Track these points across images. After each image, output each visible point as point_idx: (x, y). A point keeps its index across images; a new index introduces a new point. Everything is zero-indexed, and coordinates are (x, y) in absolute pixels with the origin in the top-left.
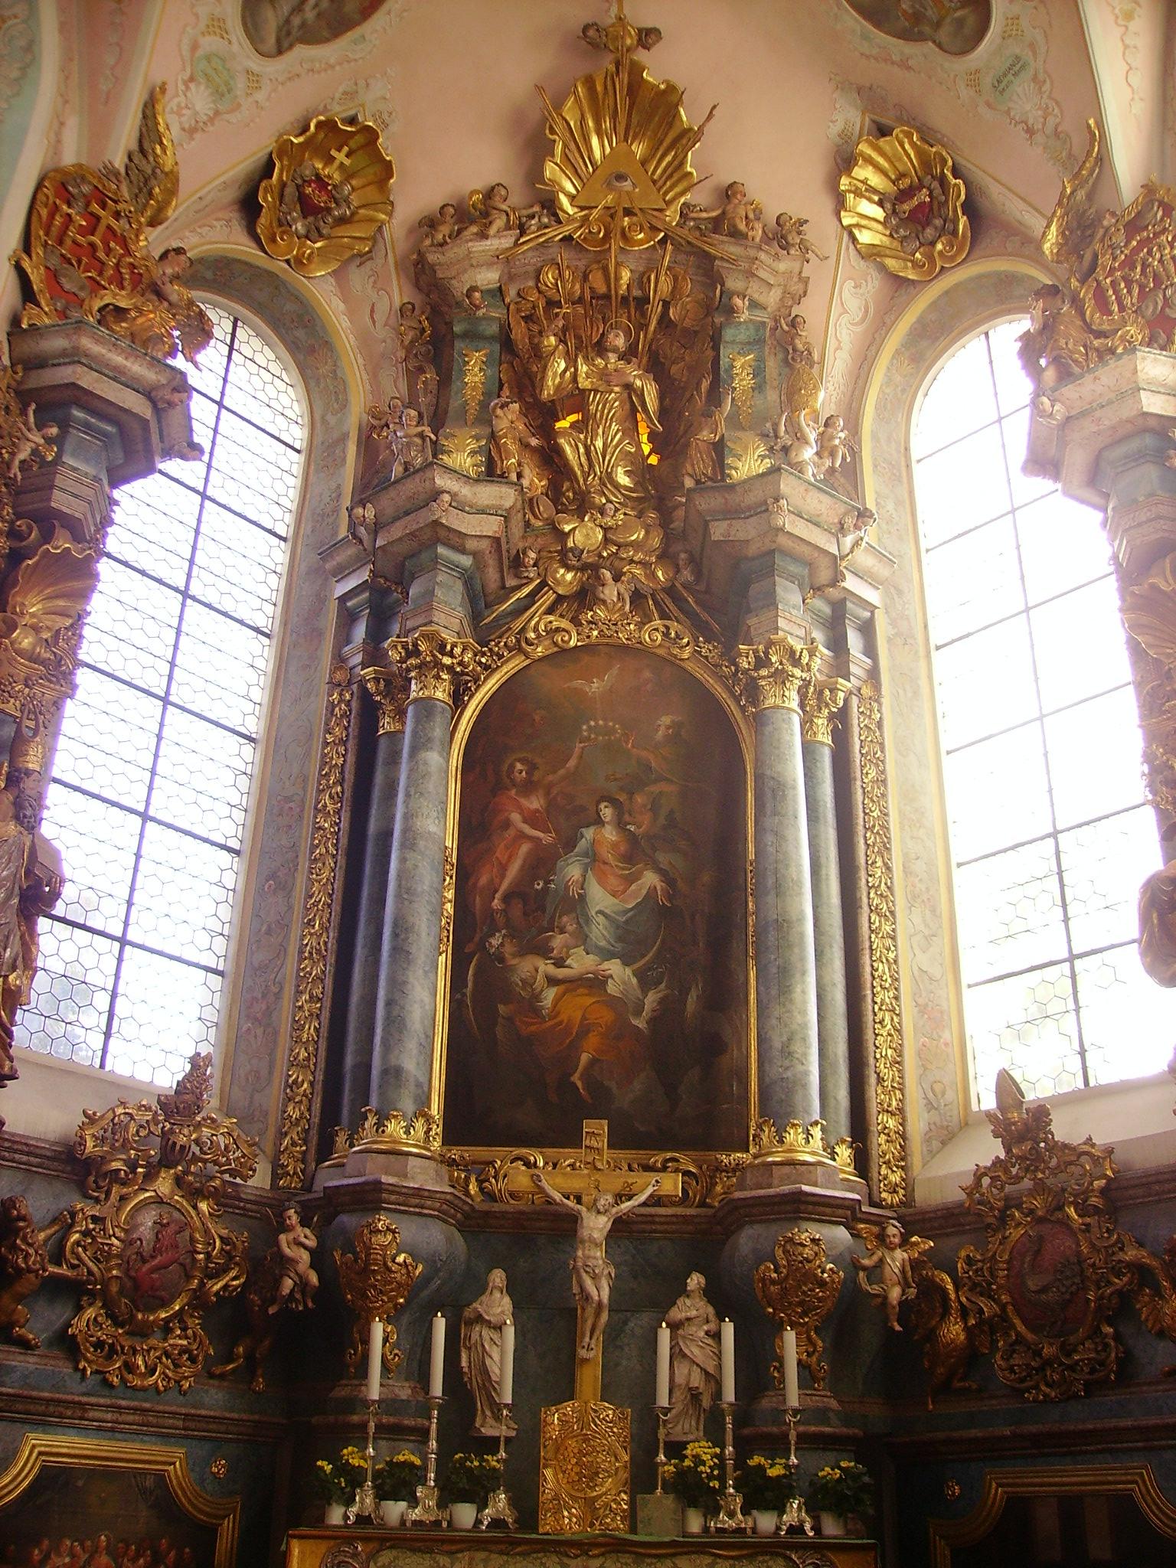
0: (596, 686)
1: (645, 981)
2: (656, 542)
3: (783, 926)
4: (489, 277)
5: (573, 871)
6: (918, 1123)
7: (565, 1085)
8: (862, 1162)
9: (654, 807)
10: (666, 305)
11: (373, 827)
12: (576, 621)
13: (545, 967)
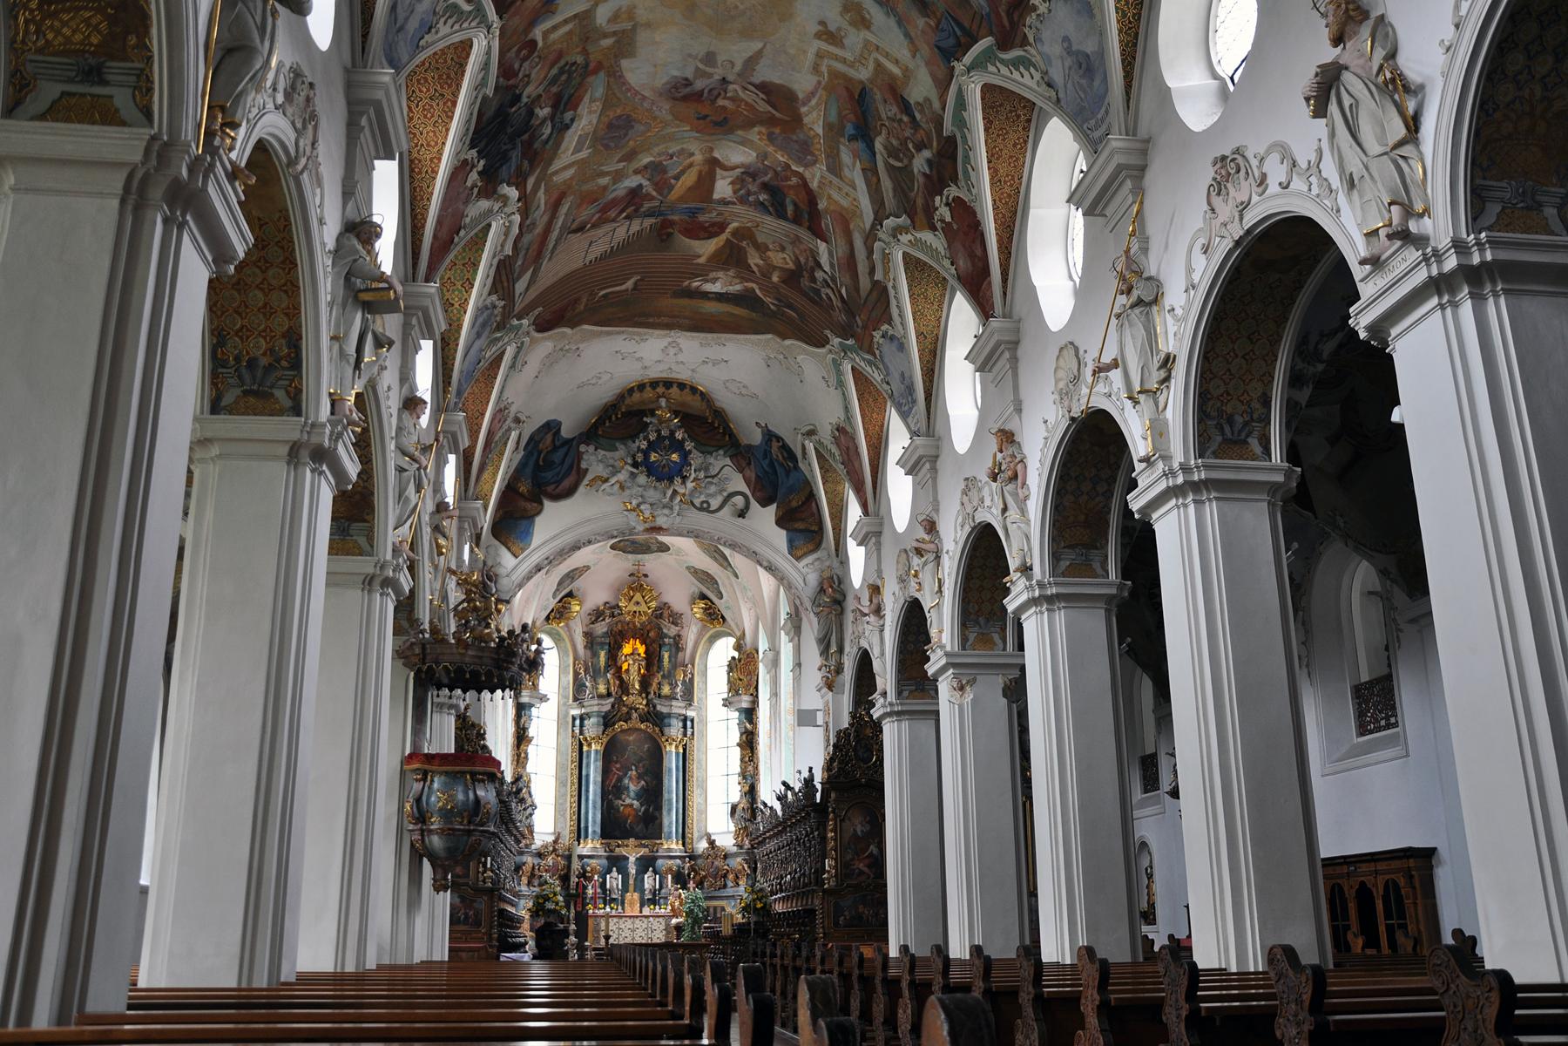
0: (631, 738)
1: (642, 805)
2: (644, 702)
3: (670, 800)
4: (605, 630)
5: (627, 781)
6: (696, 835)
7: (625, 827)
8: (684, 845)
9: (644, 766)
10: (648, 632)
11: (584, 773)
12: (626, 722)
13: (621, 802)
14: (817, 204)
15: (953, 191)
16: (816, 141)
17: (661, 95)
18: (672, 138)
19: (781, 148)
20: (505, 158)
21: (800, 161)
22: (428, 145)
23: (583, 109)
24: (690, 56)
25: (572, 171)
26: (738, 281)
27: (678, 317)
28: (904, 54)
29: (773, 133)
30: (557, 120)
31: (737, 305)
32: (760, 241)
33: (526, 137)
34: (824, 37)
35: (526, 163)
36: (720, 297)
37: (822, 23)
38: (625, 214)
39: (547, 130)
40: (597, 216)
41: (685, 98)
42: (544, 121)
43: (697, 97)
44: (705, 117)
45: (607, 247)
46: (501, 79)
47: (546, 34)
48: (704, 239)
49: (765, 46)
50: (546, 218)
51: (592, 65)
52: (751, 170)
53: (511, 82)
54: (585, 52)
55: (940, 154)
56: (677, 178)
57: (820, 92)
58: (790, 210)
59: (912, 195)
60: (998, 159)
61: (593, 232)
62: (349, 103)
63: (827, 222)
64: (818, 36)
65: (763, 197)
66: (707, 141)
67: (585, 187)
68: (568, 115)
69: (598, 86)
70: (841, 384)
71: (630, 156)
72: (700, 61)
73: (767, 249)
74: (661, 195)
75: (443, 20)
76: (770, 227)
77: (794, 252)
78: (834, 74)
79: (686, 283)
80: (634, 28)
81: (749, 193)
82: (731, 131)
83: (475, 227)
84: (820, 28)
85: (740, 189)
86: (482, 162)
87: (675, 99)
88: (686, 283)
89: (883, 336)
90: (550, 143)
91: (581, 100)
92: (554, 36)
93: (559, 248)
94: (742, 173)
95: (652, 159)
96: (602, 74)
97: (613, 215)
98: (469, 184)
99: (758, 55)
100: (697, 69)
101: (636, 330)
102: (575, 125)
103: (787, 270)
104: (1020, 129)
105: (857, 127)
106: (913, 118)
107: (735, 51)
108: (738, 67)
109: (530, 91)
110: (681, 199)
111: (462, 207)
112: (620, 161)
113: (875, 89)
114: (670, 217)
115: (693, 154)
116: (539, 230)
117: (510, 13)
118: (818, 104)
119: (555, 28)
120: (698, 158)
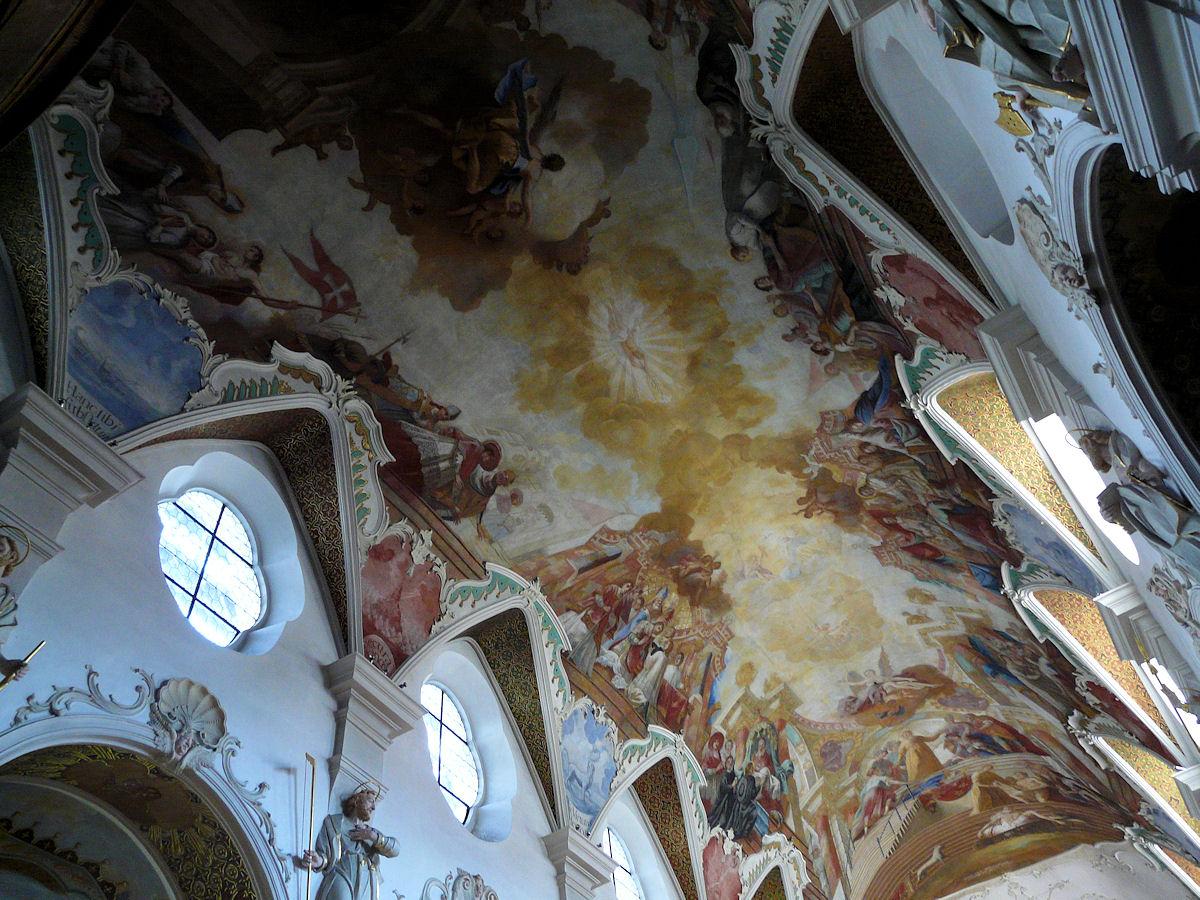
15: (1081, 681)
16: (974, 689)
17: (842, 717)
18: (874, 740)
19: (956, 707)
20: (751, 819)
21: (976, 707)
22: (676, 842)
23: (793, 753)
25: (818, 801)
26: (1015, 814)
27: (998, 862)
28: (970, 602)
30: (778, 772)
31: (1033, 832)
33: (759, 796)
34: (914, 621)
35: (775, 813)
36: (1016, 832)
37: (905, 613)
38: (887, 808)
39: (775, 782)
40: (866, 819)
41: (861, 709)
42: (767, 778)
43: (867, 705)
44: (886, 714)
45: (893, 837)
46: (709, 771)
47: (724, 724)
48: (962, 796)
49: (883, 649)
50: (824, 841)
51: (776, 725)
53: (718, 768)
54: (763, 719)
55: (1051, 656)
56: (903, 764)
57: (946, 657)
58: (1002, 744)
59: (1064, 693)
60: (1088, 639)
61: (873, 832)
62: (553, 861)
63: (1035, 740)
65: (977, 745)
67: (841, 803)
68: (786, 765)
69: (792, 735)
70: (1164, 866)
71: (856, 767)
75: (627, 761)
76: (1004, 765)
77: (1036, 774)
78: (944, 640)
79: (979, 834)
82: (911, 713)
83: (754, 881)
84: (906, 618)
85: (956, 748)
86: (731, 833)
88: (979, 834)
89: (1149, 812)
90: (786, 788)
92: (731, 723)
93: (854, 857)
95: (874, 760)
96: (788, 726)
98: (728, 851)
101: (972, 887)
102: (796, 767)
103: (1042, 789)
104: (1088, 607)
105: (990, 666)
106: (1014, 641)
108: (878, 671)
109: (739, 768)
110: (917, 776)
111: (733, 871)
113: (976, 635)
114: (923, 793)
115: (900, 743)
116: (824, 850)
117: (685, 727)
119: (728, 718)
120: (906, 743)
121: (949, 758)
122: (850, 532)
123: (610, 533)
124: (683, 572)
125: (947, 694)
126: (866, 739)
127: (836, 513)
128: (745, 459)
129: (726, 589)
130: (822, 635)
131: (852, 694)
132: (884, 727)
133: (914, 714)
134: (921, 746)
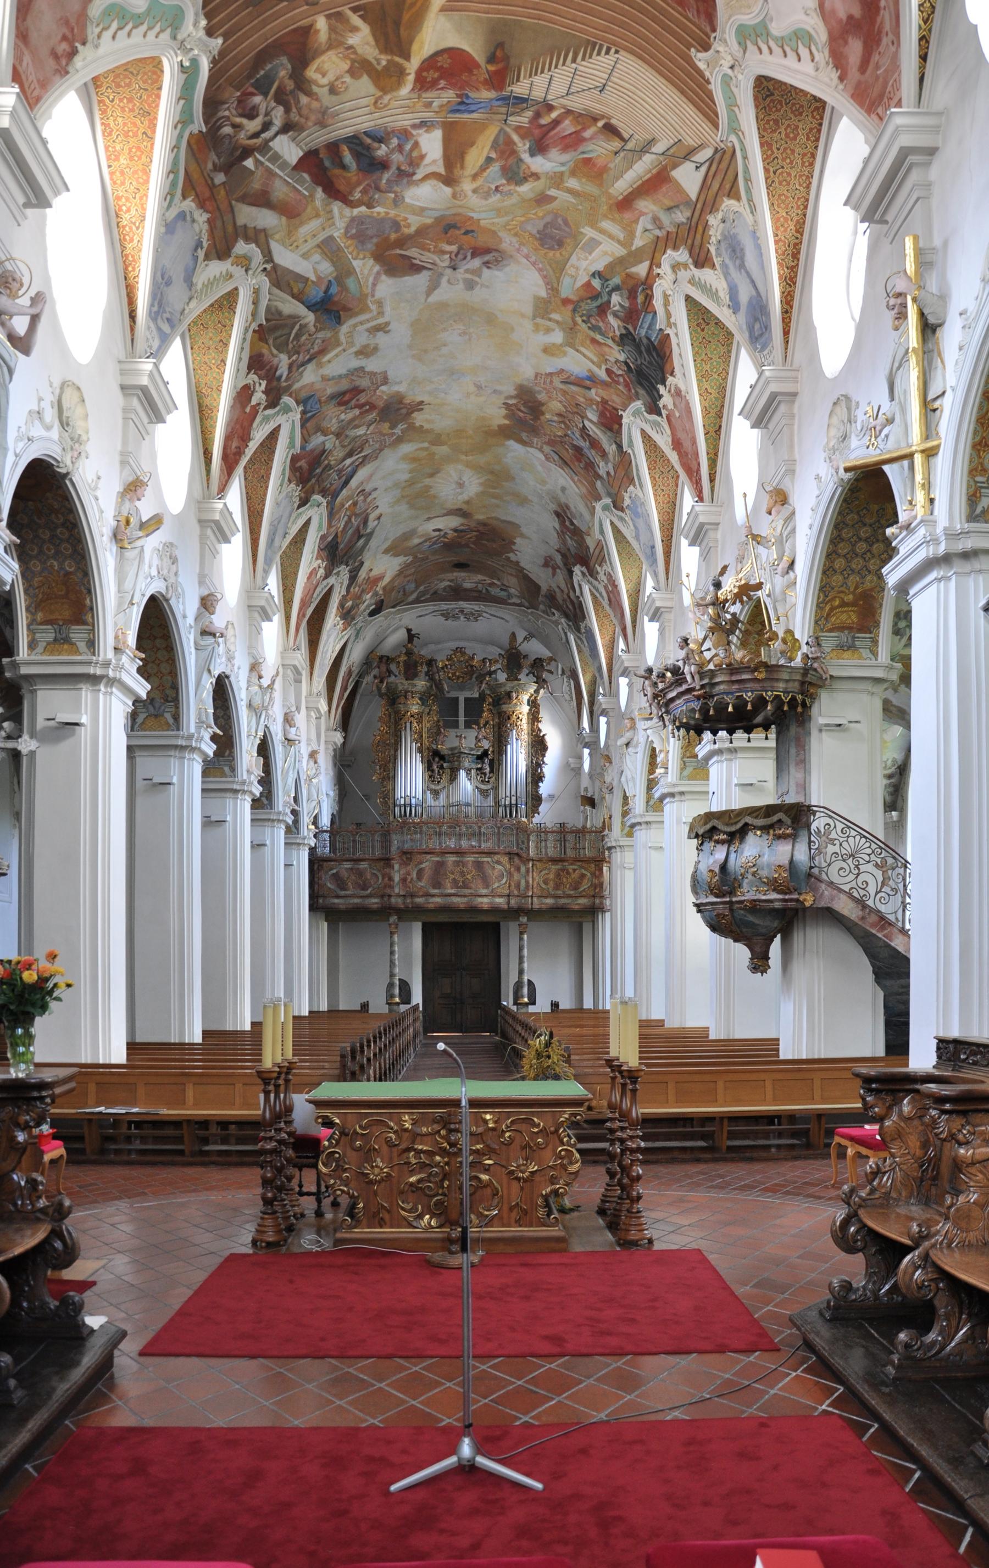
14: (324, 191)
16: (355, 253)
17: (511, 256)
18: (499, 212)
23: (583, 279)
24: (487, 287)
29: (396, 232)
32: (365, 78)
38: (554, 115)
40: (587, 134)
41: (488, 251)
43: (476, 252)
44: (467, 233)
51: (571, 307)
52: (405, 181)
56: (489, 160)
57: (369, 290)
58: (348, 157)
61: (597, 108)
64: (387, 324)
66: (460, 206)
67: (591, 188)
71: (542, 199)
72: (477, 283)
73: (352, 72)
74: (506, 134)
78: (365, 309)
80: (534, 317)
81: (400, 148)
82: (438, 220)
85: (411, 150)
87: (496, 250)
91: (583, 286)
94: (414, 174)
95: (518, 189)
96: (564, 295)
97: (567, 122)
99: (429, 292)
100: (480, 276)
107: (448, 291)
108: (444, 280)
110: (481, 127)
112: (552, 199)
114: (492, 94)
115: (475, 191)
118: (367, 280)
120: (467, 186)
121: (426, 136)
122: (398, 392)
123: (547, 459)
124: (529, 417)
125: (386, 239)
126: (506, 219)
127: (401, 402)
128: (439, 435)
129: (514, 393)
130: (471, 330)
131: (485, 270)
132: (479, 220)
133: (436, 219)
134: (452, 172)
